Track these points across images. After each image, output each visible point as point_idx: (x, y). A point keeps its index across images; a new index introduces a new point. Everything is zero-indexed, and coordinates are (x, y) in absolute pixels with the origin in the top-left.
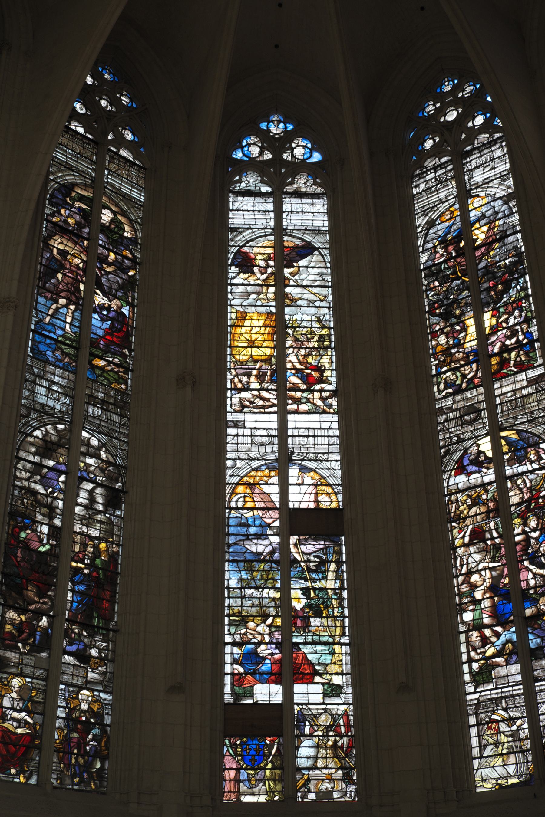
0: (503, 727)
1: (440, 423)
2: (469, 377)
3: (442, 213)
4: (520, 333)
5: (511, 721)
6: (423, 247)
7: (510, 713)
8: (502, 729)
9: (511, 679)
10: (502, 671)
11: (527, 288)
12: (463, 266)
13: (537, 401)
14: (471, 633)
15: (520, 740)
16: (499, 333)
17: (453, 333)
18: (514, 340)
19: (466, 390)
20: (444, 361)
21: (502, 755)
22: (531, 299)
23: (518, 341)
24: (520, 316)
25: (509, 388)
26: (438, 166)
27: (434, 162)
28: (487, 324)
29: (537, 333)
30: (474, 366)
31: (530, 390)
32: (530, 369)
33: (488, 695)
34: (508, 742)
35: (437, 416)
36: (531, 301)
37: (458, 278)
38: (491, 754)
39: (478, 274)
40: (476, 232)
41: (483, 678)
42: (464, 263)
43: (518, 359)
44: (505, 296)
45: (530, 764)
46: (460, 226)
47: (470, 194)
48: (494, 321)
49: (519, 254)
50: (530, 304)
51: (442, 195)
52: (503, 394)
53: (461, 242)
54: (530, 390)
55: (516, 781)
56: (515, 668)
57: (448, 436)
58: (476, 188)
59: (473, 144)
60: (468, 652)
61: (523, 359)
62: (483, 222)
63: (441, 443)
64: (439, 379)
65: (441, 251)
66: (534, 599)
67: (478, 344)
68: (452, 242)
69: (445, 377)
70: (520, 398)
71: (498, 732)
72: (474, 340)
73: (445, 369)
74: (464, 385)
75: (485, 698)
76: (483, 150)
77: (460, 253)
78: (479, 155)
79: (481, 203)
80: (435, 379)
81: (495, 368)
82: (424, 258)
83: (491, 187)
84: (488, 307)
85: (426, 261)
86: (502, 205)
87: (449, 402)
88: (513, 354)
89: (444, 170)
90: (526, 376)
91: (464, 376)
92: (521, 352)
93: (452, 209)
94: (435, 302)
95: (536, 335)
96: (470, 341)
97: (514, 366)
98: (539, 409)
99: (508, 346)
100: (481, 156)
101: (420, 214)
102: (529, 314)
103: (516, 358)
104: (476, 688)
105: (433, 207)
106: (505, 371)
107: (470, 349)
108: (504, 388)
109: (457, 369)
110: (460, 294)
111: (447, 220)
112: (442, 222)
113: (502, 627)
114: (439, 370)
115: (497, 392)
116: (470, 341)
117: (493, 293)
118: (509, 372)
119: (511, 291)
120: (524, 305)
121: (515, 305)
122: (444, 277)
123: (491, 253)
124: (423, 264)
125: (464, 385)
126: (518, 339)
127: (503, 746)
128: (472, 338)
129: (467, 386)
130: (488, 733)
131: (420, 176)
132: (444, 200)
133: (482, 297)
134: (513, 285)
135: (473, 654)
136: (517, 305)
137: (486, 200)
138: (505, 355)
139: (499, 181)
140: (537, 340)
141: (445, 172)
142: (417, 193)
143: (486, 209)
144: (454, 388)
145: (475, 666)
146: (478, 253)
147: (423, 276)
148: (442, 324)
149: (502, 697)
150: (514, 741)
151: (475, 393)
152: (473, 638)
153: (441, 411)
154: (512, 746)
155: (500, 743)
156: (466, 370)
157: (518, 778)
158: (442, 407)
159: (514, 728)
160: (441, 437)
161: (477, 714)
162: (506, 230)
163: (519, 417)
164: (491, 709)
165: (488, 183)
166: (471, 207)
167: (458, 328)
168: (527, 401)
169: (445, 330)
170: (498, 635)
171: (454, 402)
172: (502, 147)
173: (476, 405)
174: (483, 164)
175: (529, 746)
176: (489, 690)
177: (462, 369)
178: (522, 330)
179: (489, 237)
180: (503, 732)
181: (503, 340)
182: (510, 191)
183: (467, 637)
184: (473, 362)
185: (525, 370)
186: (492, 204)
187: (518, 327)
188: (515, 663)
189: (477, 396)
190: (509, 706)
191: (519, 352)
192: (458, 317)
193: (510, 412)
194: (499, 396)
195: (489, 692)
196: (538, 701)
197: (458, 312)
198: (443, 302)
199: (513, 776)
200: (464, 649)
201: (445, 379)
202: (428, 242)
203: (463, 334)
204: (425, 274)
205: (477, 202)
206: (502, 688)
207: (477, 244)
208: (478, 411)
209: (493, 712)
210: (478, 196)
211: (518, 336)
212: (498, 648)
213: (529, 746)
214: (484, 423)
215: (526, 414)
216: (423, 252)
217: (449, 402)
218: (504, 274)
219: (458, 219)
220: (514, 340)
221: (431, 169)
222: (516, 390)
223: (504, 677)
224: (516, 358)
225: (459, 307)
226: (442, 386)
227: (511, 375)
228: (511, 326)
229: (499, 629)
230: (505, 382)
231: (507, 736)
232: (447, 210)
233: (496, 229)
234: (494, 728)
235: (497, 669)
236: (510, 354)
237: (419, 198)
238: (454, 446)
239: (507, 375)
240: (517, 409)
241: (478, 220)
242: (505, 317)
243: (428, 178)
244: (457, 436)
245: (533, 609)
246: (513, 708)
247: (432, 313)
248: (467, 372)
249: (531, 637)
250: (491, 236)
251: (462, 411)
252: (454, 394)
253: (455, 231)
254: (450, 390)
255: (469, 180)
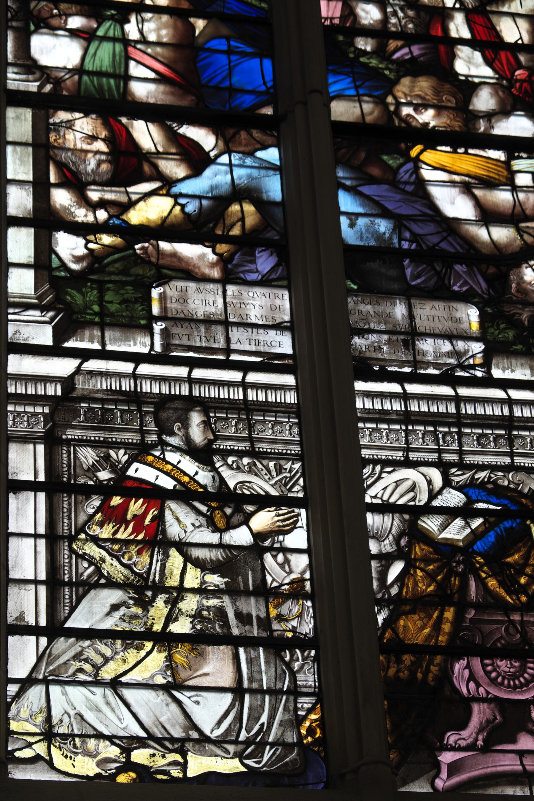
0: (181, 521)
5: (226, 505)
7: (226, 473)
8: (174, 530)
9: (240, 339)
10: (205, 301)
14: (63, 116)
15: (264, 592)
21: (165, 640)
33: (121, 375)
34: (202, 591)
38: (108, 624)
41: (101, 301)
45: (305, 703)
55: (230, 766)
56: (262, 303)
60: (40, 187)
66: (375, 74)
71: (157, 540)
75: (102, 384)
104: (60, 334)
113: (217, 132)
127: (173, 603)
130: (106, 532)
135: (61, 198)
145: (69, 247)
149: (191, 402)
150: (232, 591)
152: (74, 139)
154: (221, 613)
155: (159, 588)
157: (240, 756)
159: (241, 536)
161: (53, 441)
164: (133, 437)
170: (197, 160)
175: (307, 627)
176: (122, 361)
180: (182, 547)
183: (42, 129)
188: (265, 282)
190: (222, 445)
195: (127, 367)
196: (365, 452)
199: (219, 742)
200: (19, 166)
206: (192, 364)
209: (141, 452)
212: (192, 207)
213: (307, 627)
223: (208, 322)
229: (204, 138)
231: (201, 565)
234: (139, 519)
235: (180, 284)
245: (367, 107)
246: (241, 454)
249: (346, 202)
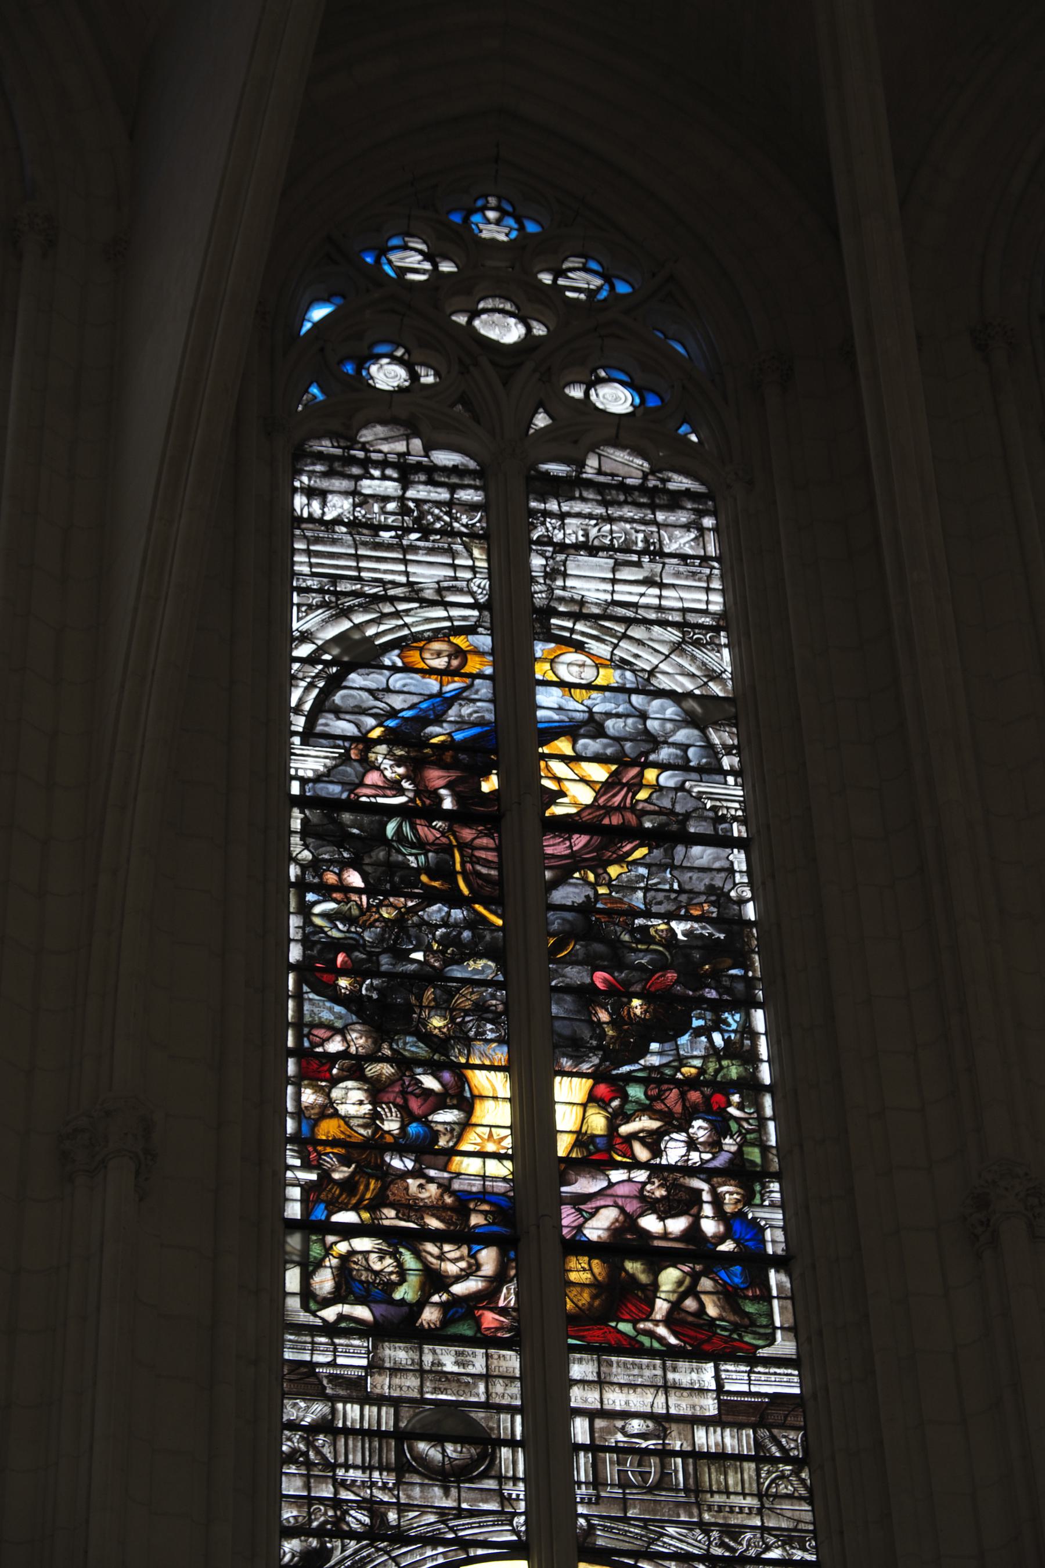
1: (294, 1426)
2: (458, 1289)
3: (416, 637)
4: (708, 1210)
6: (312, 718)
11: (751, 1058)
12: (486, 863)
13: (760, 1496)
16: (616, 1175)
17: (404, 1093)
18: (677, 1225)
19: (437, 1336)
20: (348, 1185)
22: (768, 1101)
23: (694, 1228)
24: (715, 1146)
25: (639, 1401)
26: (419, 467)
27: (400, 447)
28: (566, 1119)
29: (780, 1236)
30: (488, 1258)
31: (730, 1441)
32: (737, 1360)
35: (284, 1395)
36: (769, 1112)
37: (454, 899)
39: (547, 923)
40: (559, 768)
42: (491, 856)
43: (690, 1304)
44: (654, 1046)
46: (490, 717)
47: (548, 626)
48: (597, 1123)
49: (729, 919)
50: (762, 1120)
51: (428, 574)
52: (603, 1413)
53: (486, 775)
54: (730, 1441)
57: (326, 1491)
58: (576, 617)
59: (582, 465)
61: (712, 1311)
62: (590, 745)
63: (289, 1514)
64: (316, 1251)
65: (393, 771)
67: (514, 1180)
68: (448, 756)
69: (342, 1247)
70: (681, 1454)
72: (499, 1157)
73: (347, 1217)
74: (430, 1316)
76: (620, 504)
77: (473, 810)
78: (600, 510)
79: (589, 675)
80: (294, 1241)
81: (577, 1300)
82: (309, 762)
83: (640, 642)
84: (578, 1059)
85: (318, 778)
86: (679, 724)
87: (353, 1358)
88: (670, 1277)
89: (444, 495)
90: (717, 1377)
91: (434, 1281)
92: (706, 1284)
93: (459, 641)
94: (336, 946)
95: (774, 1242)
96: (483, 1155)
97: (669, 1321)
98: (763, 1529)
99: (646, 1234)
100: (610, 520)
101: (315, 599)
102: (754, 1154)
103: (683, 1297)
105: (376, 599)
106: (625, 1327)
107: (476, 1186)
108: (615, 1395)
109: (413, 1239)
110: (460, 960)
111: (431, 672)
112: (407, 669)
114: (319, 1213)
115: (579, 1397)
116: (483, 1155)
117: (604, 1016)
118: (646, 1341)
119: (684, 1040)
120: (733, 1111)
121: (694, 1096)
122: (391, 867)
123: (614, 871)
124: (304, 781)
125: (430, 1316)
126: (694, 1228)
128: (491, 1147)
129: (446, 1321)
131: (335, 467)
132: (429, 594)
133: (554, 1010)
134: (696, 1023)
136: (702, 1099)
137: (609, 677)
138: (633, 1267)
139: (673, 635)
140: (779, 1263)
141: (450, 504)
142: (311, 519)
143: (609, 707)
144: (381, 1309)
146: (555, 847)
147: (296, 824)
148: (358, 1041)
151: (478, 1365)
153: (307, 1380)
156: (451, 1260)
158: (312, 1365)
160: (292, 1486)
162: (687, 816)
163: (671, 1530)
165: (628, 622)
166: (542, 670)
167: (430, 1082)
168: (711, 1476)
169: (373, 1070)
171: (375, 1366)
172: (701, 530)
173: (479, 1415)
174: (611, 548)
177: (431, 1248)
178: (717, 1202)
179: (609, 810)
181: (631, 1207)
182: (716, 689)
184: (486, 1240)
185: (718, 1357)
186: (637, 700)
187: (697, 1183)
189: (487, 1377)
191: (695, 1277)
192: (439, 1044)
193: (633, 1494)
194: (592, 1415)
197: (437, 1022)
198: (373, 957)
201: (346, 1258)
202: (338, 712)
203: (448, 1116)
204: (305, 822)
205: (571, 667)
207: (557, 810)
208: (487, 1444)
210: (579, 647)
211: (697, 1218)
214: (506, 1500)
215: (705, 1528)
216: (309, 736)
217: (353, 1358)
218: (661, 966)
219: (484, 689)
220: (677, 1225)
221: (384, 464)
222: (668, 1417)
224: (683, 1297)
225: (443, 1006)
226: (324, 1282)
227: (651, 1353)
228: (670, 1168)
230: (620, 1368)
232: (437, 635)
233: (643, 795)
236: (655, 1271)
237: (318, 540)
238: (353, 1545)
239: (632, 1348)
240: (664, 1495)
241: (572, 730)
242: (645, 1123)
243: (368, 487)
244: (370, 1506)
247: (316, 973)
248: (452, 1269)
250: (620, 809)
251: (406, 1412)
252: (377, 1332)
253: (462, 723)
254: (362, 1312)
255: (551, 574)
